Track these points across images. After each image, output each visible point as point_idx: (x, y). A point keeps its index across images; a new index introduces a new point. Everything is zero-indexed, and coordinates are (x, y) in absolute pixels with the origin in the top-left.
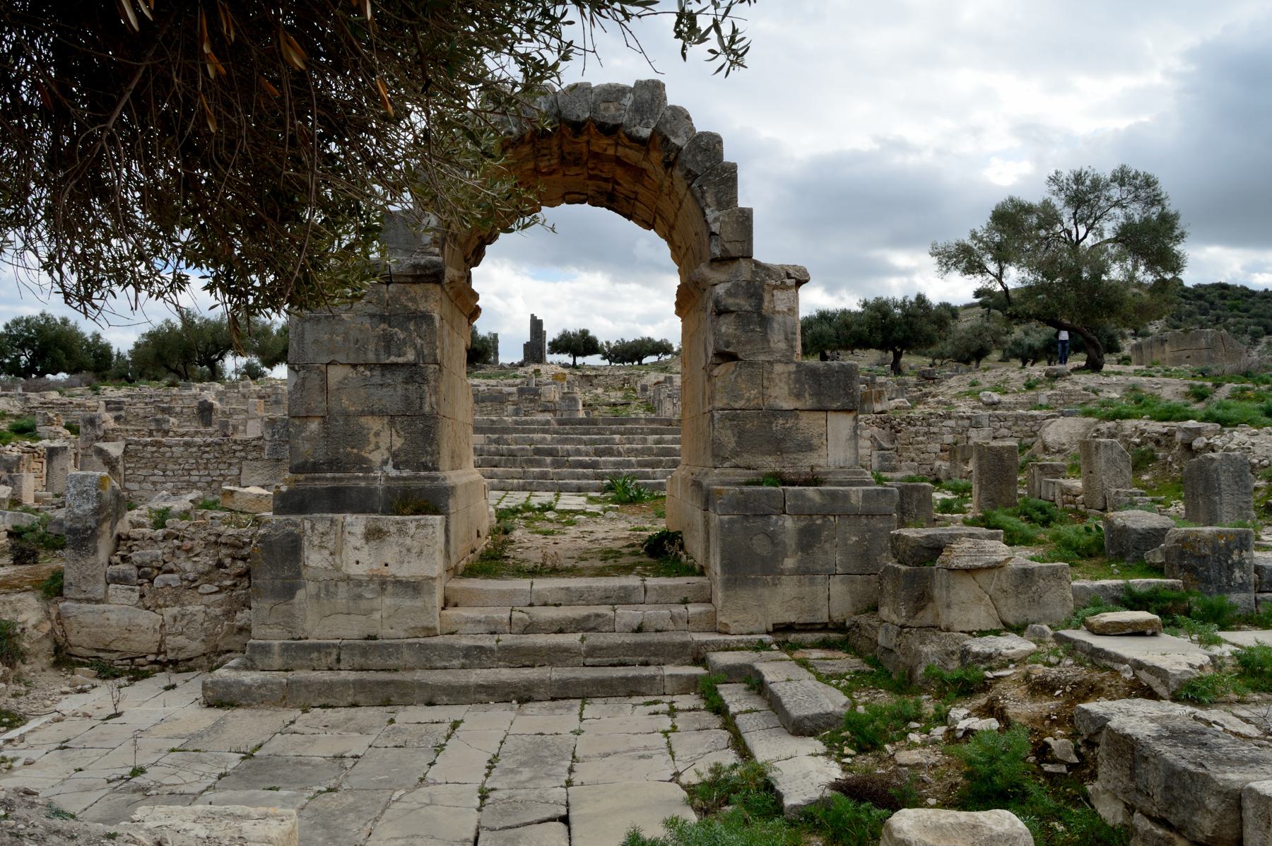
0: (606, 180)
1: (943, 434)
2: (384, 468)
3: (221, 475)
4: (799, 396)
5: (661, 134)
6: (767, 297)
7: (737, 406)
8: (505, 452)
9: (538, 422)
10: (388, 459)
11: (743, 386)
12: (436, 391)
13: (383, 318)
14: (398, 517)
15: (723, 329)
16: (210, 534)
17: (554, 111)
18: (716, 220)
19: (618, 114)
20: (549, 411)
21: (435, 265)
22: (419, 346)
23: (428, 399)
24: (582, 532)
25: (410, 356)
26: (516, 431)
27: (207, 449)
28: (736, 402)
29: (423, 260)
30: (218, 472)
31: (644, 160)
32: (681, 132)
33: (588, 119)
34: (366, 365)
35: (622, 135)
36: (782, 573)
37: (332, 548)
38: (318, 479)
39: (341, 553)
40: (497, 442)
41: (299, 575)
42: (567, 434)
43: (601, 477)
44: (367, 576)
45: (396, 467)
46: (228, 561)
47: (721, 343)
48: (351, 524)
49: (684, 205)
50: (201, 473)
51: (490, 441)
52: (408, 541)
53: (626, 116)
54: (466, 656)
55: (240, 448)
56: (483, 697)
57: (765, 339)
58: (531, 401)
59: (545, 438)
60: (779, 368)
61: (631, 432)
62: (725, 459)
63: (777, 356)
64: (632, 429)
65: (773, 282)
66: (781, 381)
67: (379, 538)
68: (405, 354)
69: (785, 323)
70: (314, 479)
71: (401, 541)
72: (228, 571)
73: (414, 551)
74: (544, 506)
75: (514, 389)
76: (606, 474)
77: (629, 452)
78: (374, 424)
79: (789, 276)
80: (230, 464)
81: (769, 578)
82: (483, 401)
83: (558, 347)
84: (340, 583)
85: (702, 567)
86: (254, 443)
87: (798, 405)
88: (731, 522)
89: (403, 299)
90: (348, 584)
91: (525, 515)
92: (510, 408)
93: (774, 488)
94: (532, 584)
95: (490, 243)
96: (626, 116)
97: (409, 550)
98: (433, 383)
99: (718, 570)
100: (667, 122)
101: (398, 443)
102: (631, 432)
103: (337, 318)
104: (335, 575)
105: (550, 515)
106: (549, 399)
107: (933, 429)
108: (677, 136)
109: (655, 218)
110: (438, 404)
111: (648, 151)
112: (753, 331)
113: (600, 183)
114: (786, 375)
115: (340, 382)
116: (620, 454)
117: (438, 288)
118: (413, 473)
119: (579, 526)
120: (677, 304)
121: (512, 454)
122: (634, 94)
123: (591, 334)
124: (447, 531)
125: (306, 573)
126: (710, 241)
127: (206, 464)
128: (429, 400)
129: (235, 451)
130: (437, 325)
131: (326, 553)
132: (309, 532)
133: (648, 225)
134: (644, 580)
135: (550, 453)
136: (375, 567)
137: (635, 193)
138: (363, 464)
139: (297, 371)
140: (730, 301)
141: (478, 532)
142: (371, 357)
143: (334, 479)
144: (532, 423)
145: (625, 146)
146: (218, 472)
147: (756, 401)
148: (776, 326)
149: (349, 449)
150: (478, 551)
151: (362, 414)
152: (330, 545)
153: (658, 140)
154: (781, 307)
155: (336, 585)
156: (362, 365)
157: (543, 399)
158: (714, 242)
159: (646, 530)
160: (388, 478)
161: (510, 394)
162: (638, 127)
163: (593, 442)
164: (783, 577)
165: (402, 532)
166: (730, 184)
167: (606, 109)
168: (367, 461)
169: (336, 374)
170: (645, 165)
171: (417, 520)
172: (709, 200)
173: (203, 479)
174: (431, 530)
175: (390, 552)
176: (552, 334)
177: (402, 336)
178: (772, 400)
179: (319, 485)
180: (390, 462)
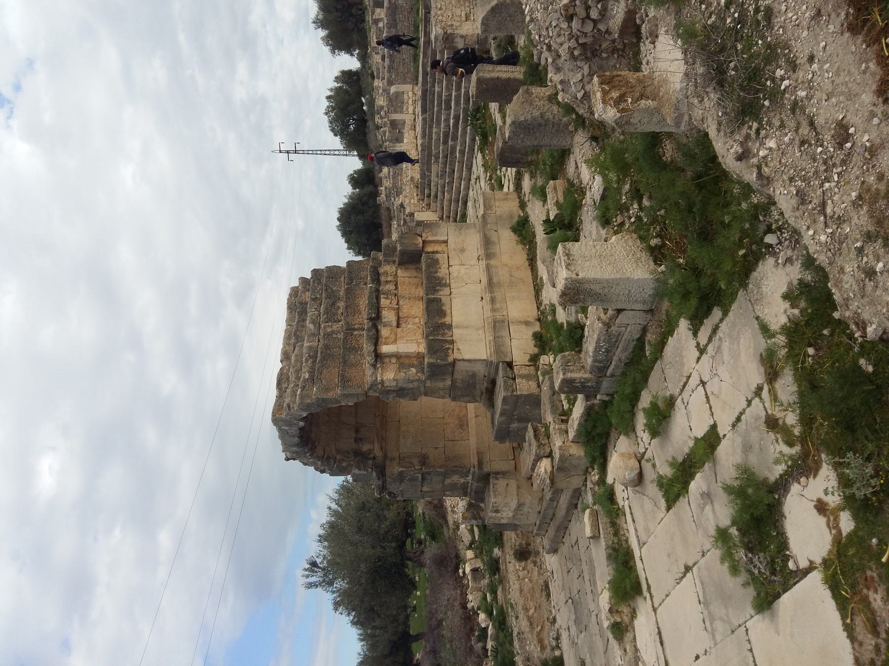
40: (437, 158)
42: (433, 114)
54: (553, 501)
56: (571, 512)
59: (436, 133)
117: (388, 463)
169: (425, 489)
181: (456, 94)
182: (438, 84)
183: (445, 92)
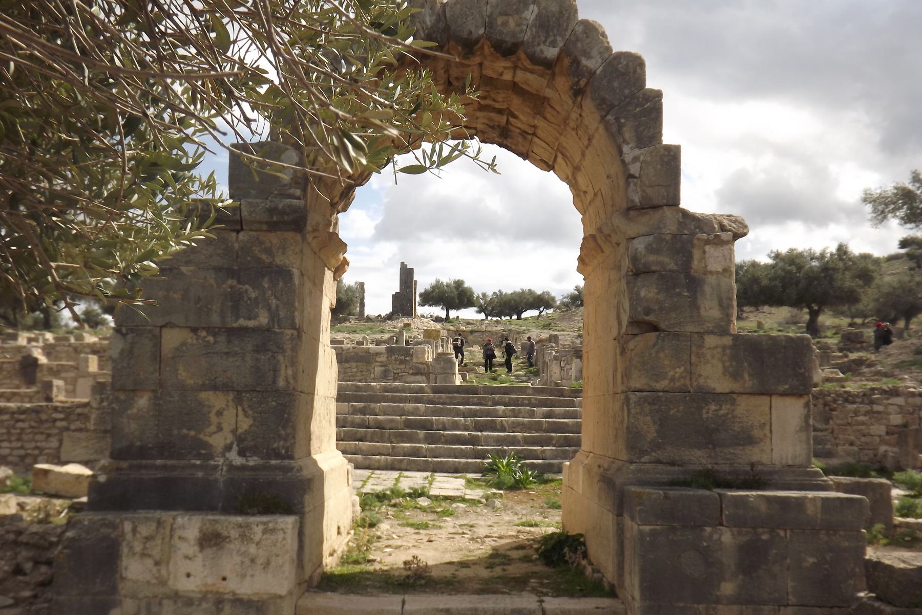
0: (500, 112)
1: (889, 414)
2: (227, 455)
3: (37, 448)
4: (735, 375)
5: (569, 54)
6: (697, 254)
7: (658, 386)
8: (372, 423)
9: (411, 390)
10: (232, 444)
11: (666, 362)
12: (293, 363)
13: (231, 273)
14: (240, 519)
15: (643, 293)
16: (8, 532)
17: (441, 25)
18: (636, 159)
19: (518, 29)
20: (422, 374)
21: (295, 210)
22: (273, 307)
23: (283, 372)
24: (461, 526)
25: (263, 319)
26: (386, 400)
27: (22, 417)
28: (657, 381)
29: (283, 203)
30: (33, 445)
31: (548, 86)
32: (594, 52)
33: (481, 37)
34: (211, 330)
35: (523, 56)
36: (718, 601)
37: (157, 557)
38: (146, 467)
39: (168, 563)
40: (363, 412)
41: (114, 590)
43: (482, 455)
44: (200, 592)
45: (241, 453)
46: (28, 566)
47: (639, 309)
48: (183, 527)
49: (594, 142)
50: (14, 444)
51: (355, 411)
52: (252, 549)
53: (529, 33)
55: (62, 416)
57: (694, 306)
58: (402, 362)
59: (417, 408)
60: (711, 341)
61: (516, 403)
62: (643, 453)
63: (710, 326)
64: (517, 399)
65: (705, 236)
66: (713, 357)
67: (216, 544)
68: (256, 317)
69: (719, 286)
70: (140, 467)
71: (243, 549)
72: (27, 579)
73: (260, 561)
74: (415, 491)
75: (383, 347)
76: (487, 451)
77: (514, 427)
78: (216, 400)
79: (723, 228)
80: (49, 435)
81: (701, 607)
82: (347, 361)
83: (430, 298)
84: (165, 602)
85: (612, 586)
86: (79, 411)
87: (736, 387)
88: (653, 533)
89: (256, 250)
90: (175, 602)
91: (393, 502)
92: (378, 370)
93: (707, 493)
94: (404, 603)
95: (360, 185)
96: (529, 33)
97: (253, 561)
98: (289, 352)
99: (637, 594)
100: (577, 40)
101: (245, 424)
102: (516, 403)
103: (175, 271)
104: (160, 590)
105: (423, 502)
106: (421, 360)
107: (876, 408)
108: (589, 57)
109: (556, 157)
110: (295, 377)
111: (553, 75)
112: (679, 294)
113: (492, 114)
114: (720, 350)
115: (177, 349)
116: (503, 430)
117: (299, 237)
118: (261, 462)
119: (457, 517)
120: (580, 259)
121: (380, 426)
122: (539, 7)
123: (466, 285)
124: (301, 534)
125: (124, 588)
126: (627, 184)
127: (20, 434)
128: (285, 372)
129: (55, 420)
130: (296, 281)
131: (149, 562)
132: (129, 536)
133: (547, 166)
134: (541, 601)
135: (423, 425)
136: (210, 581)
137: (535, 127)
138: (202, 450)
139: (124, 335)
140: (652, 258)
141: (339, 528)
142: (215, 319)
143: (164, 467)
144: (403, 390)
145: (526, 69)
146: (33, 445)
147: (682, 381)
148: (707, 289)
149: (185, 431)
150: (339, 552)
151: (203, 388)
152: (156, 552)
153: (567, 61)
154: (715, 266)
155: (160, 604)
156: (204, 328)
157: (415, 360)
158: (632, 187)
159: (536, 525)
160: (231, 467)
161: (378, 354)
162: (542, 47)
163: (474, 414)
164: (720, 607)
165: (245, 537)
166: (653, 116)
167: (505, 24)
168: (207, 446)
169: (172, 339)
170: (548, 93)
171: (265, 524)
172: (627, 135)
173: (16, 452)
174: (280, 536)
175: (229, 562)
176: (423, 282)
177: (253, 295)
178: (702, 381)
179: (145, 474)
180: (235, 445)
181: (520, 438)
182: (511, 410)
183: (507, 421)
